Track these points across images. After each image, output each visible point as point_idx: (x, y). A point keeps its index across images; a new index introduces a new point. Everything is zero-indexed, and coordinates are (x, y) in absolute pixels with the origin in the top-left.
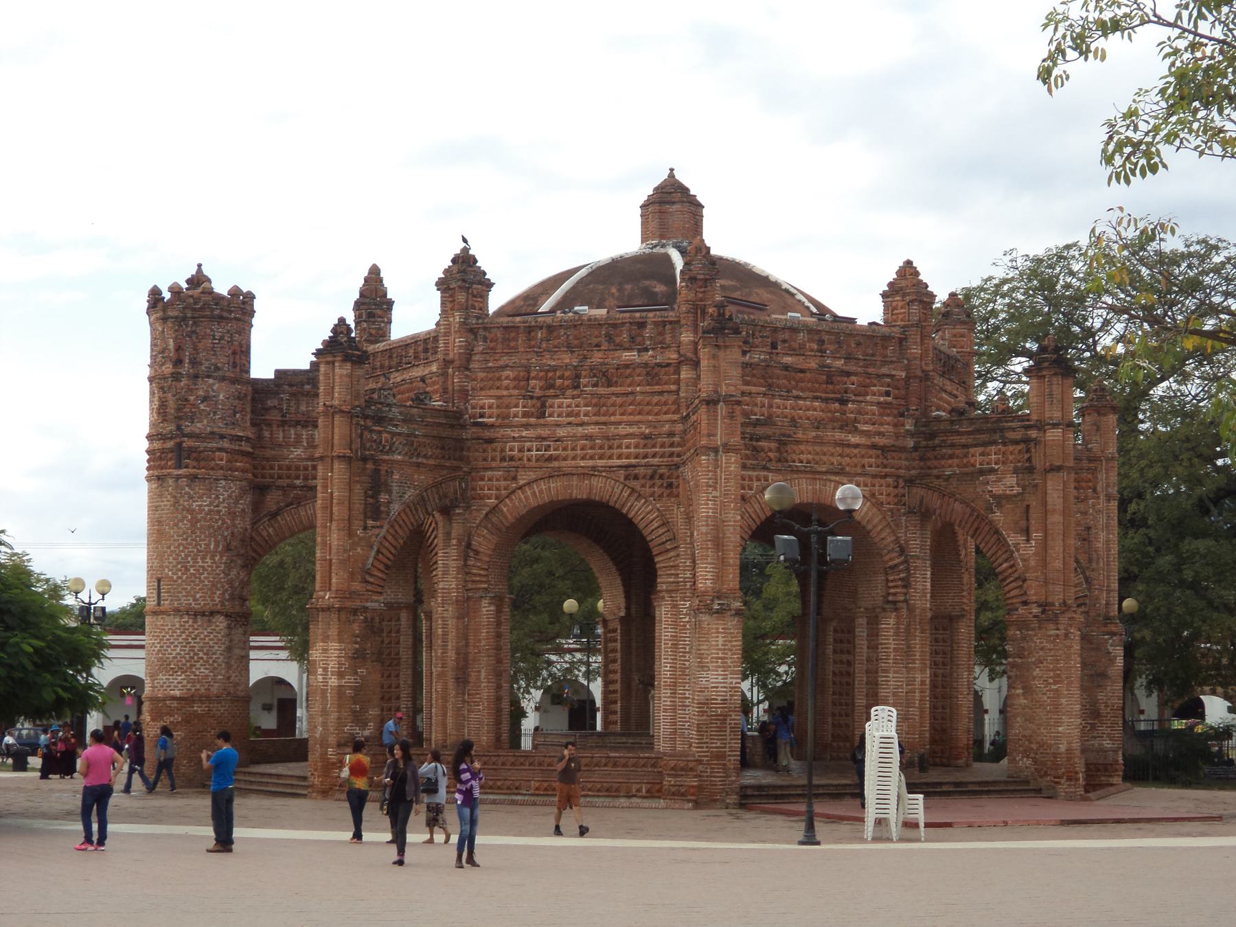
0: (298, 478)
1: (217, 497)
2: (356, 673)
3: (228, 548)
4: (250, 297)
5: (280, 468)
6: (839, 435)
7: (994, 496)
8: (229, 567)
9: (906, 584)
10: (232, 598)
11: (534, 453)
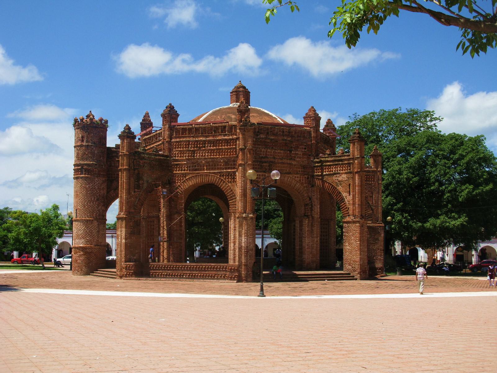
1: (94, 184)
2: (132, 239)
3: (98, 200)
4: (106, 122)
6: (289, 161)
7: (339, 181)
9: (312, 210)
10: (99, 215)
11: (191, 168)
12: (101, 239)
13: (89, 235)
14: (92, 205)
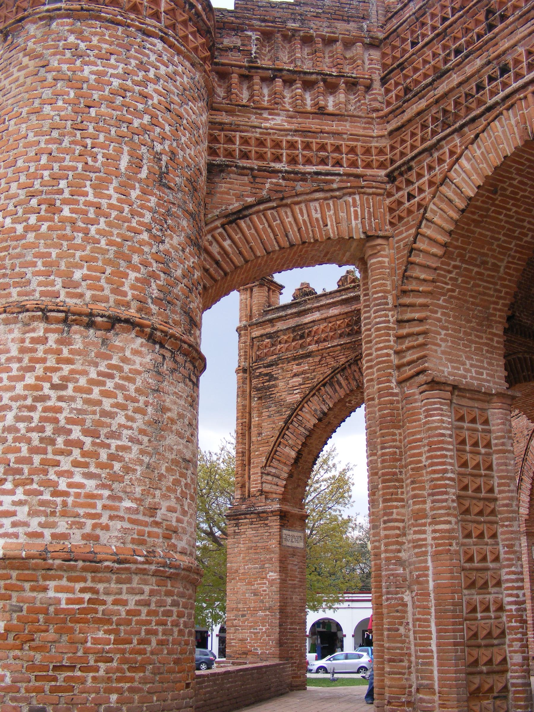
0: (277, 159)
3: (161, 179)
5: (245, 141)
8: (163, 220)
12: (173, 503)
13: (76, 453)
14: (111, 206)
